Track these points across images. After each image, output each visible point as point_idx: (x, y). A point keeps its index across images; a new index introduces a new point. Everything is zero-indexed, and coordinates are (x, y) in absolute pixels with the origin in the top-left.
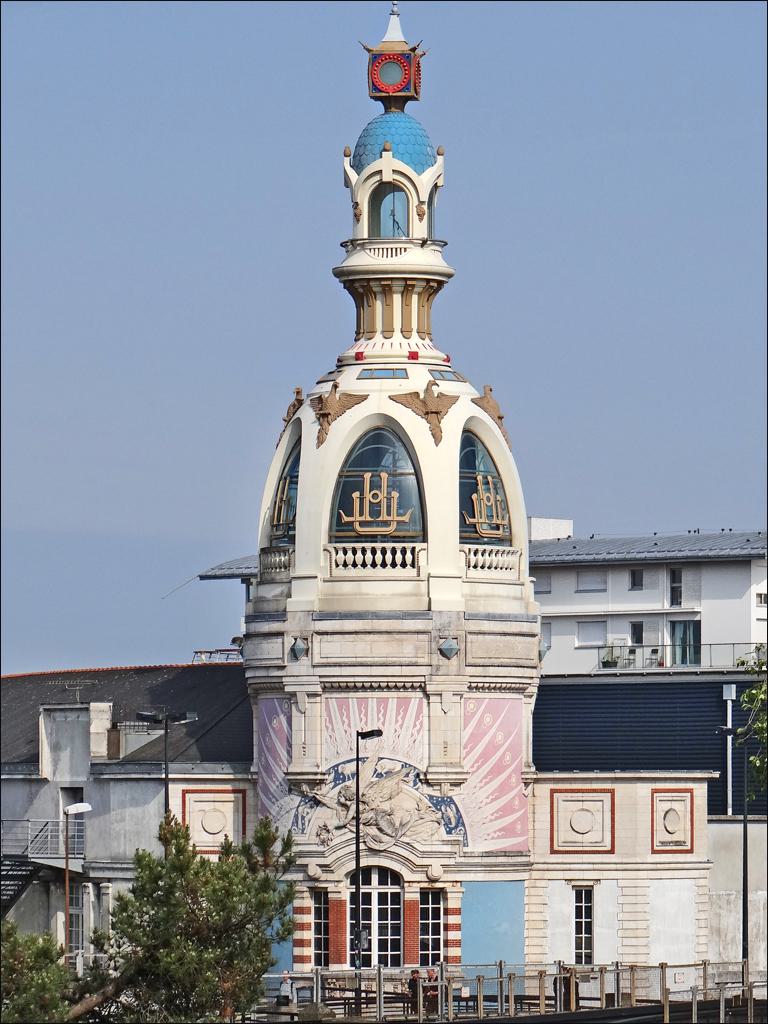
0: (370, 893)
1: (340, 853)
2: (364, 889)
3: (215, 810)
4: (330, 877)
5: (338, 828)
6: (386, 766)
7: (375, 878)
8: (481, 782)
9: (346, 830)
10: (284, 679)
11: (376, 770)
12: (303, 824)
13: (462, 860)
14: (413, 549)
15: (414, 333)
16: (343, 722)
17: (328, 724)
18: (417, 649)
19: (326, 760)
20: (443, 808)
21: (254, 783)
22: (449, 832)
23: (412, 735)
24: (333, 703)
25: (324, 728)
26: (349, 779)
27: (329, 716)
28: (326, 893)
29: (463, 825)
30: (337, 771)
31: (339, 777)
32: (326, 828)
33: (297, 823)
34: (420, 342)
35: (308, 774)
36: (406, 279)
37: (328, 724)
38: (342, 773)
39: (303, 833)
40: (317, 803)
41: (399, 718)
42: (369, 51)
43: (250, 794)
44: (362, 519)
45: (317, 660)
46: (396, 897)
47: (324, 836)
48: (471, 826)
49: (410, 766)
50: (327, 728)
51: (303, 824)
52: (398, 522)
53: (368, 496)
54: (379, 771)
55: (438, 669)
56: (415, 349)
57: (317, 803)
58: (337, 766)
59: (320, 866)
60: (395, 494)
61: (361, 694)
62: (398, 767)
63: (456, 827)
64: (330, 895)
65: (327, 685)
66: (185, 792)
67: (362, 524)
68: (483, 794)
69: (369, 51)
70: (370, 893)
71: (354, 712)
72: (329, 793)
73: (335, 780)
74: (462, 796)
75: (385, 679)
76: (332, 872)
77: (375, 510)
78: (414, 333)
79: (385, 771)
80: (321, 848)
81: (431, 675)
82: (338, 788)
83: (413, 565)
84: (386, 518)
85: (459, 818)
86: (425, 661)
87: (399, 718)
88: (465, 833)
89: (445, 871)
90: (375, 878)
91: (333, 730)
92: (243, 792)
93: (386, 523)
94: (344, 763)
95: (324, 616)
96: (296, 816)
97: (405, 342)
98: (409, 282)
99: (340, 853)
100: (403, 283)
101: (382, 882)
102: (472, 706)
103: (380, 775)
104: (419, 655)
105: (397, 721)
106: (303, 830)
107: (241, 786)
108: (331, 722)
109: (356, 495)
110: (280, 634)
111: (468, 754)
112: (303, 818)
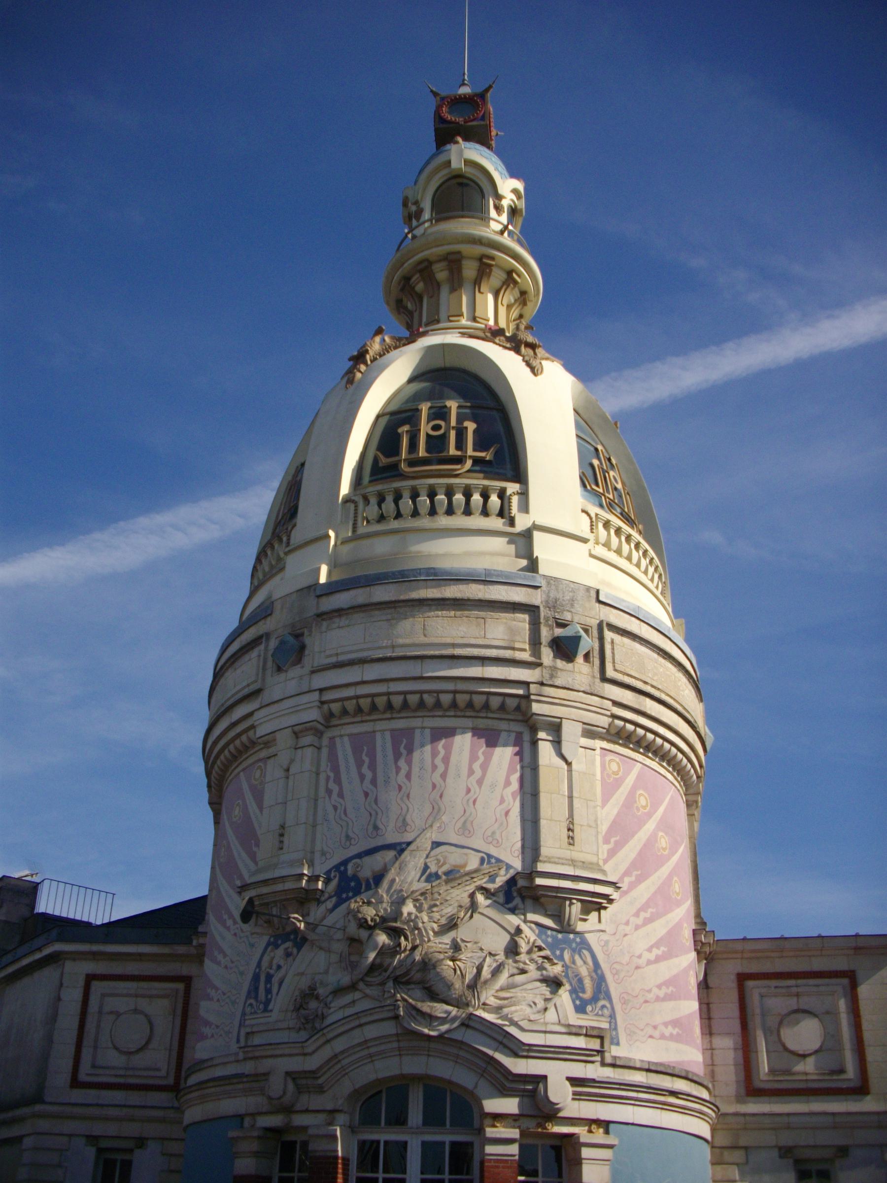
0: (406, 1143)
1: (339, 1045)
2: (384, 1135)
3: (136, 1011)
5: (339, 991)
6: (454, 857)
7: (415, 1115)
8: (637, 915)
9: (357, 995)
10: (257, 716)
11: (426, 867)
13: (607, 1073)
14: (502, 494)
16: (362, 777)
17: (332, 785)
18: (512, 631)
19: (323, 854)
20: (567, 956)
21: (199, 958)
22: (580, 1009)
23: (502, 801)
24: (344, 748)
25: (322, 791)
26: (368, 888)
27: (336, 769)
28: (305, 1144)
29: (609, 997)
30: (343, 875)
33: (257, 989)
37: (332, 785)
38: (355, 877)
39: (266, 1010)
40: (300, 940)
41: (476, 766)
42: (435, 94)
44: (412, 456)
46: (462, 1156)
47: (313, 1004)
48: (625, 1003)
49: (498, 861)
50: (329, 792)
51: (268, 991)
52: (477, 461)
53: (425, 428)
54: (433, 868)
55: (552, 676)
57: (300, 940)
58: (345, 863)
60: (471, 426)
62: (473, 863)
63: (595, 999)
64: (312, 1147)
65: (336, 707)
66: (90, 978)
67: (411, 463)
68: (641, 941)
69: (435, 94)
70: (406, 1143)
71: (385, 756)
74: (604, 937)
75: (450, 686)
76: (321, 1090)
77: (437, 443)
79: (445, 868)
80: (304, 1035)
81: (542, 684)
82: (344, 906)
83: (501, 514)
84: (453, 451)
85: (600, 981)
86: (526, 656)
87: (476, 766)
88: (613, 1016)
89: (575, 1093)
90: (415, 1115)
91: (341, 795)
92: (187, 980)
93: (459, 460)
94: (359, 856)
96: (256, 978)
99: (339, 1045)
101: (433, 1119)
102: (614, 767)
103: (432, 877)
104: (517, 645)
105: (471, 772)
106: (267, 1002)
107: (185, 970)
108: (338, 781)
109: (406, 428)
111: (612, 853)
112: (269, 978)
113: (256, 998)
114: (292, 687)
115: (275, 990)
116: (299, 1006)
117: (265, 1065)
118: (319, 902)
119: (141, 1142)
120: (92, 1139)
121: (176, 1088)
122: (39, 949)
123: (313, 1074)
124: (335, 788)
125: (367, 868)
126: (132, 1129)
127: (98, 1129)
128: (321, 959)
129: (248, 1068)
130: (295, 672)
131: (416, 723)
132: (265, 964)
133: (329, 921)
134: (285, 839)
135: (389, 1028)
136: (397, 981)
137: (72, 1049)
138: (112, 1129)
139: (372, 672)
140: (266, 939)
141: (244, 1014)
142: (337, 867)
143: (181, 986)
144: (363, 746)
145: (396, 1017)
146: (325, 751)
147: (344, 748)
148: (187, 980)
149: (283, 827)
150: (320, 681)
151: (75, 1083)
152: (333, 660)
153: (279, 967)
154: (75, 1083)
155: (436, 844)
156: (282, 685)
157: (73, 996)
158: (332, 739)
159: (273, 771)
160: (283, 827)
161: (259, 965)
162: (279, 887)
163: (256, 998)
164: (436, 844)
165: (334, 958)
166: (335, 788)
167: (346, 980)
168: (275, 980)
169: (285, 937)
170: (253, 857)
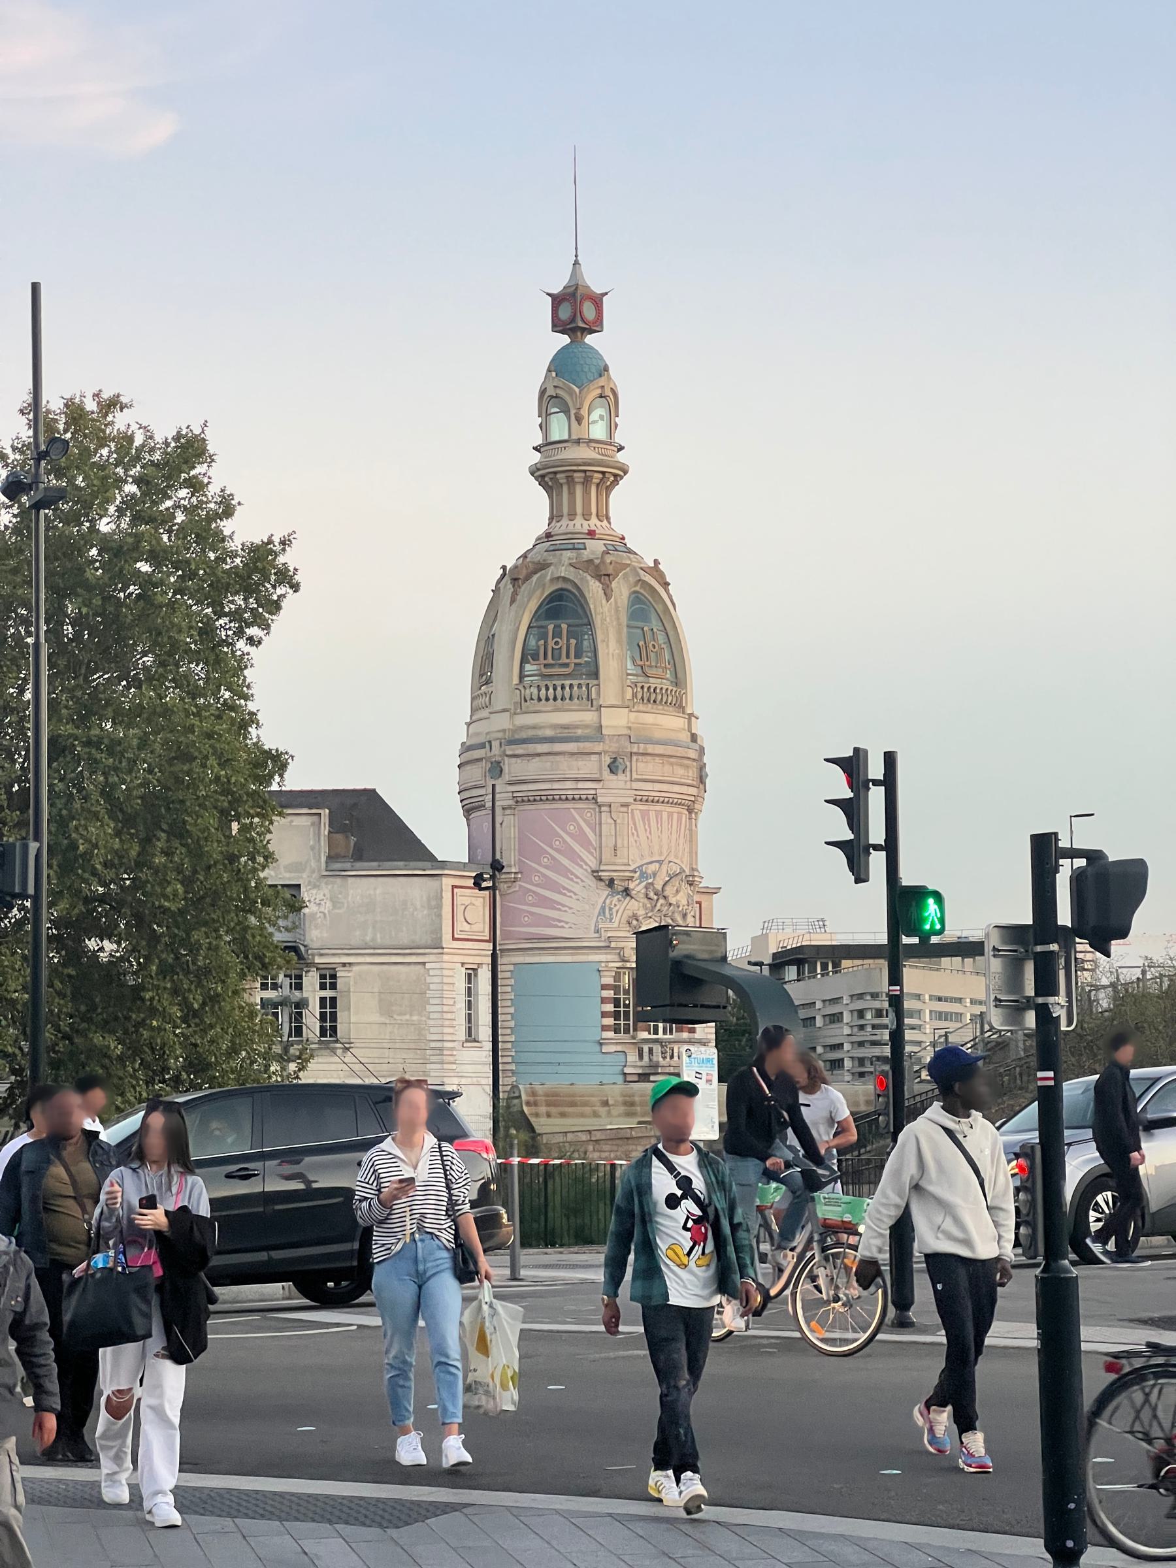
12: (611, 915)
15: (594, 516)
24: (637, 814)
27: (635, 824)
31: (644, 875)
34: (599, 524)
36: (585, 471)
45: (635, 776)
47: (635, 922)
51: (611, 915)
56: (593, 528)
61: (658, 807)
66: (454, 887)
78: (594, 516)
96: (603, 908)
97: (585, 523)
100: (582, 475)
106: (611, 919)
108: (636, 829)
112: (610, 909)
114: (621, 785)
117: (621, 945)
120: (463, 964)
126: (478, 960)
130: (621, 776)
132: (608, 902)
133: (638, 889)
139: (657, 786)
144: (645, 815)
147: (637, 814)
150: (636, 785)
151: (454, 939)
154: (454, 939)
156: (617, 782)
157: (447, 896)
168: (614, 910)
170: (591, 854)
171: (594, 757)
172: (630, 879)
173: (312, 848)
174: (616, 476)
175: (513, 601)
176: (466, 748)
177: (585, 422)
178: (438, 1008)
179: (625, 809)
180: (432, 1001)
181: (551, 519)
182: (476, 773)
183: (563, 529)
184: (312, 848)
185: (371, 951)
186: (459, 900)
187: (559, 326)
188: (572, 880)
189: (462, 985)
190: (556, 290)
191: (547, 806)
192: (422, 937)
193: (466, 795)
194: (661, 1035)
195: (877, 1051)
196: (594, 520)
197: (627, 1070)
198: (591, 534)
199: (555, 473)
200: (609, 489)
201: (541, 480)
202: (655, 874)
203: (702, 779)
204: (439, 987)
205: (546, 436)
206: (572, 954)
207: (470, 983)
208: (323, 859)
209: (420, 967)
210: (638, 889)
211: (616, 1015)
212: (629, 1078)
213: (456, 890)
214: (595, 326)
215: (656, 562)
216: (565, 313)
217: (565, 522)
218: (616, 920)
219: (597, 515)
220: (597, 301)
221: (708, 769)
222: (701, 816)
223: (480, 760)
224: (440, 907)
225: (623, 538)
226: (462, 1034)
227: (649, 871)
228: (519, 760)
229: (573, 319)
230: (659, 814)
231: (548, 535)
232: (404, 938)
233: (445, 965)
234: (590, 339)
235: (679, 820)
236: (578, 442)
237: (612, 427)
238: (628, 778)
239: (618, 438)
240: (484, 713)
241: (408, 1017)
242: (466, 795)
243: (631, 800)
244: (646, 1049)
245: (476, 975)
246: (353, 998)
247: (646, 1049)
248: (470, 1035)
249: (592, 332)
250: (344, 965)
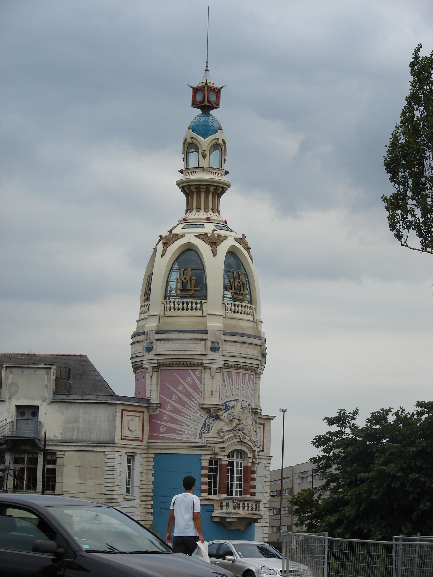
4: (223, 453)
9: (231, 432)
10: (204, 361)
17: (223, 383)
32: (222, 431)
33: (205, 427)
34: (212, 214)
35: (217, 405)
36: (206, 185)
37: (223, 383)
38: (229, 406)
43: (146, 413)
44: (235, 291)
45: (225, 354)
50: (222, 385)
51: (209, 428)
58: (227, 402)
59: (220, 448)
61: (237, 371)
72: (224, 415)
73: (226, 409)
75: (249, 365)
76: (224, 451)
91: (225, 386)
95: (157, 332)
96: (204, 425)
98: (208, 187)
100: (205, 187)
106: (208, 431)
110: (205, 340)
112: (208, 425)
113: (205, 429)
115: (210, 428)
116: (218, 433)
117: (213, 445)
118: (221, 410)
119: (136, 454)
120: (126, 453)
121: (142, 441)
122: (107, 400)
123: (224, 448)
124: (224, 384)
125: (231, 404)
126: (135, 451)
127: (128, 450)
128: (223, 423)
129: (209, 445)
130: (217, 353)
131: (240, 371)
132: (207, 421)
134: (213, 394)
135: (238, 440)
136: (238, 430)
137: (120, 429)
138: (130, 451)
139: (237, 359)
140: (206, 416)
141: (201, 432)
142: (225, 403)
143: (142, 414)
145: (240, 438)
146: (221, 374)
147: (226, 374)
148: (143, 412)
149: (212, 391)
152: (227, 354)
153: (211, 423)
154: (122, 439)
155: (243, 401)
158: (223, 371)
159: (207, 375)
160: (212, 391)
161: (205, 421)
162: (215, 406)
163: (205, 429)
164: (243, 401)
165: (226, 424)
166: (224, 384)
167: (230, 429)
169: (213, 417)
170: (199, 395)
171: (202, 342)
172: (220, 409)
173: (46, 386)
174: (223, 188)
175: (163, 255)
176: (135, 335)
177: (207, 158)
178: (111, 477)
179: (219, 371)
180: (108, 472)
181: (187, 211)
182: (140, 348)
183: (193, 217)
184: (46, 386)
185: (76, 444)
186: (125, 418)
187: (195, 104)
188: (188, 408)
189: (125, 464)
190: (195, 85)
191: (176, 368)
192: (104, 437)
193: (134, 360)
194: (234, 496)
195: (254, 505)
196: (210, 212)
197: (214, 515)
198: (208, 219)
199: (190, 186)
200: (220, 195)
201: (183, 189)
202: (233, 407)
203: (264, 355)
204: (112, 465)
205: (187, 164)
206: (186, 449)
207: (130, 463)
208: (52, 392)
209: (101, 453)
210: (224, 415)
211: (210, 484)
212: (214, 520)
213: (124, 412)
214: (216, 105)
215: (244, 236)
216: (199, 98)
217: (194, 212)
218: (212, 431)
219: (212, 210)
220: (217, 91)
221: (267, 351)
222: (262, 377)
223: (141, 341)
224: (114, 421)
225: (226, 222)
226: (123, 491)
227: (231, 406)
228: (162, 342)
229: (203, 101)
230: (237, 374)
231: (185, 219)
232: (94, 437)
233: (116, 453)
234: (212, 112)
235: (249, 377)
236: (203, 169)
237: (222, 161)
238: (221, 354)
239: (226, 167)
240: (145, 316)
241: (94, 481)
242: (134, 360)
243: (222, 366)
244: (225, 503)
245: (133, 459)
246: (65, 469)
247: (225, 503)
248: (129, 492)
249: (213, 108)
250: (61, 451)
